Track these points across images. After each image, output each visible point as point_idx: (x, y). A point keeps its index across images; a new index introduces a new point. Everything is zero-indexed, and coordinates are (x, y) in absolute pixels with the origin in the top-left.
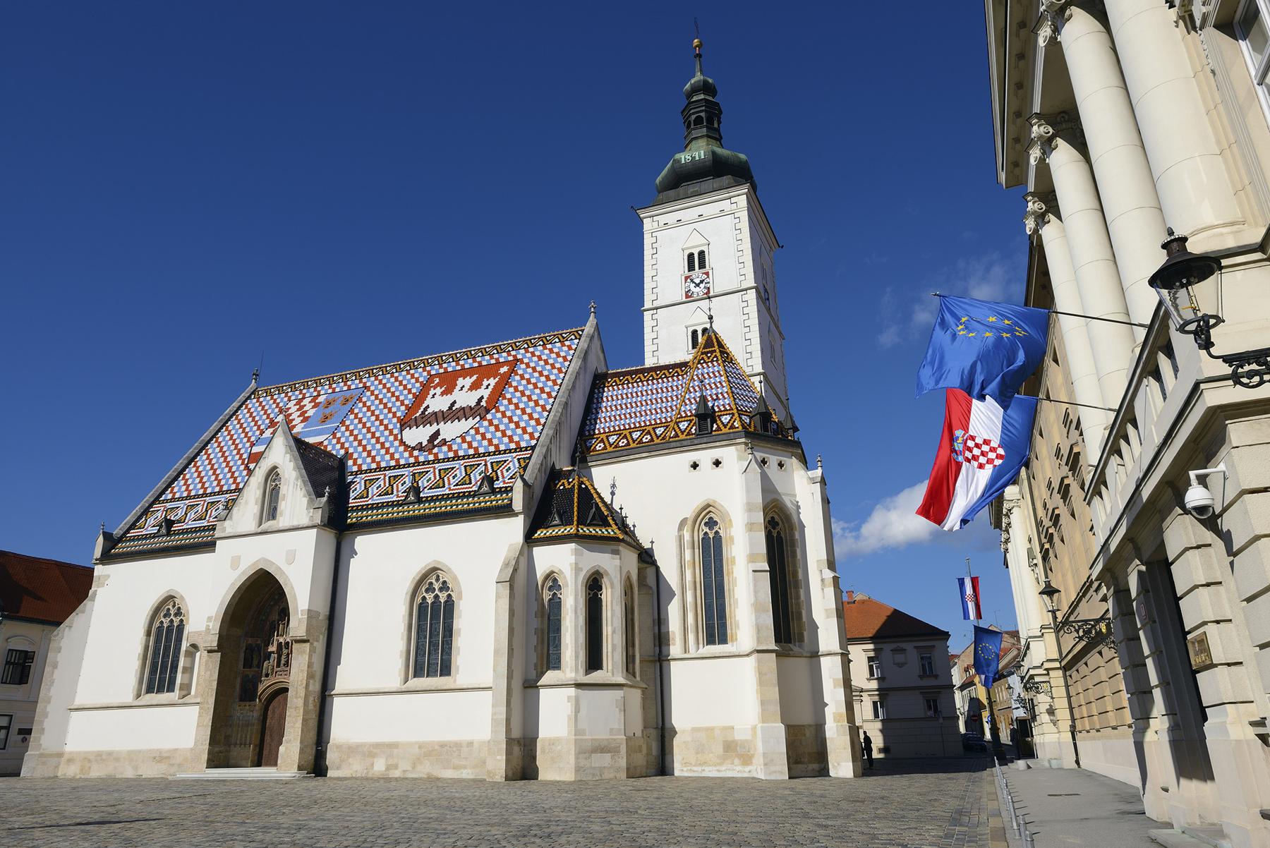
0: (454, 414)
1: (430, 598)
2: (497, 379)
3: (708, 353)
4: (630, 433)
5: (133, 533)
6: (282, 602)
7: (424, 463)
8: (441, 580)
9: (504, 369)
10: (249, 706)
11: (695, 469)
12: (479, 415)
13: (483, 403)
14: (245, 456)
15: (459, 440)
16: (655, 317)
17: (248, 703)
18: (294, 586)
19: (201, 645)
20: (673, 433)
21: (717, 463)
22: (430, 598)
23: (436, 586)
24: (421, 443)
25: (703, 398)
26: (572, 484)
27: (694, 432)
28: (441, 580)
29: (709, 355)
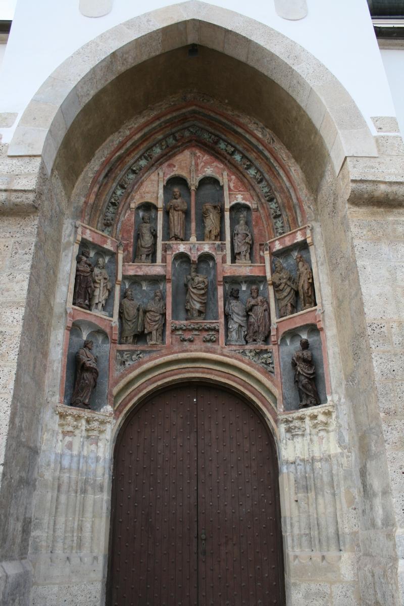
6: (171, 166)
10: (88, 421)
17: (86, 413)
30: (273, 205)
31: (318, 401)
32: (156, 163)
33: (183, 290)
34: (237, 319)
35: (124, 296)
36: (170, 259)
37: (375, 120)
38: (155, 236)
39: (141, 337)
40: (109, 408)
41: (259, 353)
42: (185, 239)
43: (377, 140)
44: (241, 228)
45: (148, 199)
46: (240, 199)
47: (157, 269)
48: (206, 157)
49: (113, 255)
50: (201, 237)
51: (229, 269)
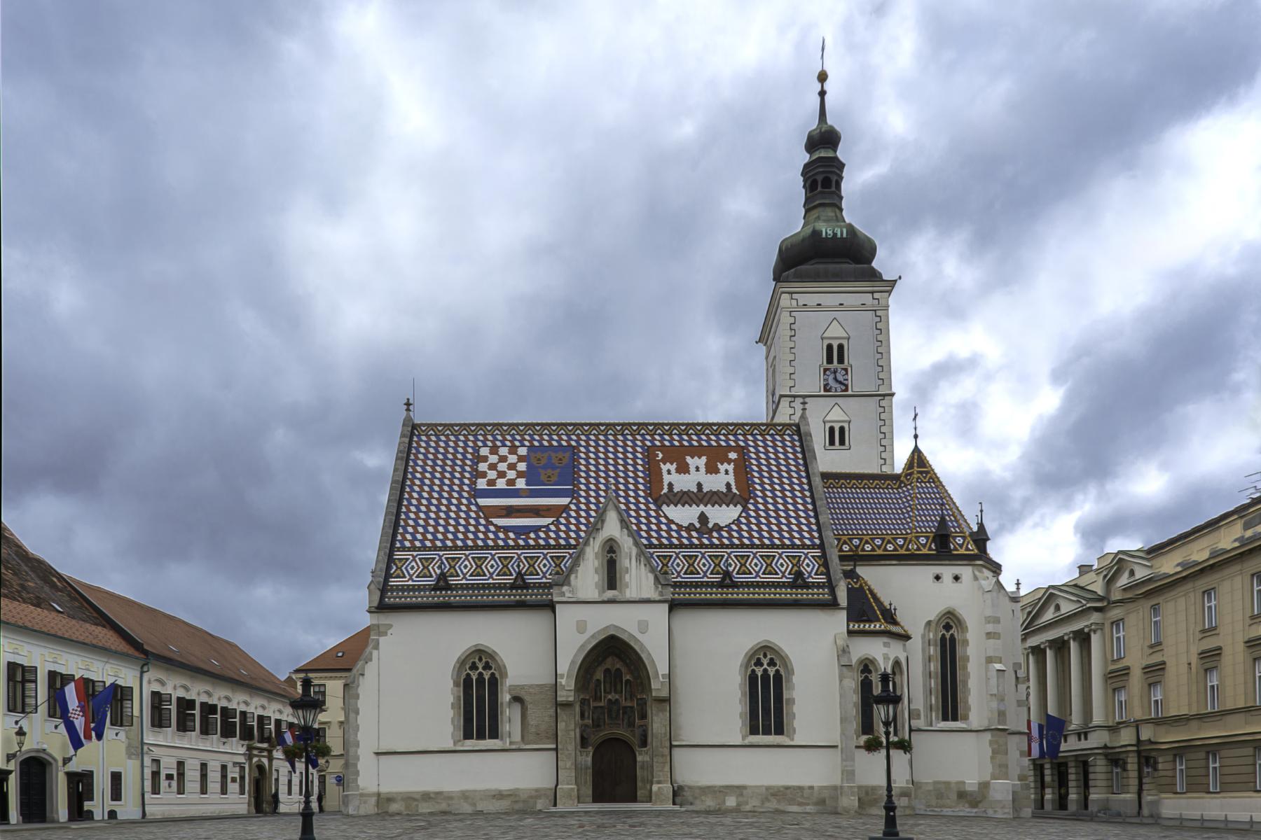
0: (699, 497)
1: (759, 671)
2: (732, 466)
3: (921, 473)
4: (871, 539)
5: (394, 582)
7: (712, 546)
8: (769, 657)
9: (733, 455)
11: (938, 580)
12: (738, 503)
13: (735, 490)
14: (473, 508)
15: (734, 527)
16: (792, 404)
17: (585, 750)
18: (651, 652)
19: (527, 698)
20: (915, 546)
21: (957, 578)
22: (759, 671)
23: (765, 662)
24: (692, 524)
25: (943, 517)
26: (859, 584)
27: (934, 548)
28: (769, 657)
29: (924, 475)
30: (639, 681)
31: (646, 747)
32: (600, 664)
33: (610, 711)
34: (626, 721)
35: (593, 713)
36: (606, 701)
37: (663, 675)
38: (601, 692)
39: (598, 726)
40: (591, 748)
41: (632, 731)
42: (610, 693)
43: (662, 682)
44: (628, 686)
45: (598, 678)
46: (628, 677)
47: (602, 704)
48: (617, 660)
49: (589, 700)
50: (616, 692)
51: (624, 703)
